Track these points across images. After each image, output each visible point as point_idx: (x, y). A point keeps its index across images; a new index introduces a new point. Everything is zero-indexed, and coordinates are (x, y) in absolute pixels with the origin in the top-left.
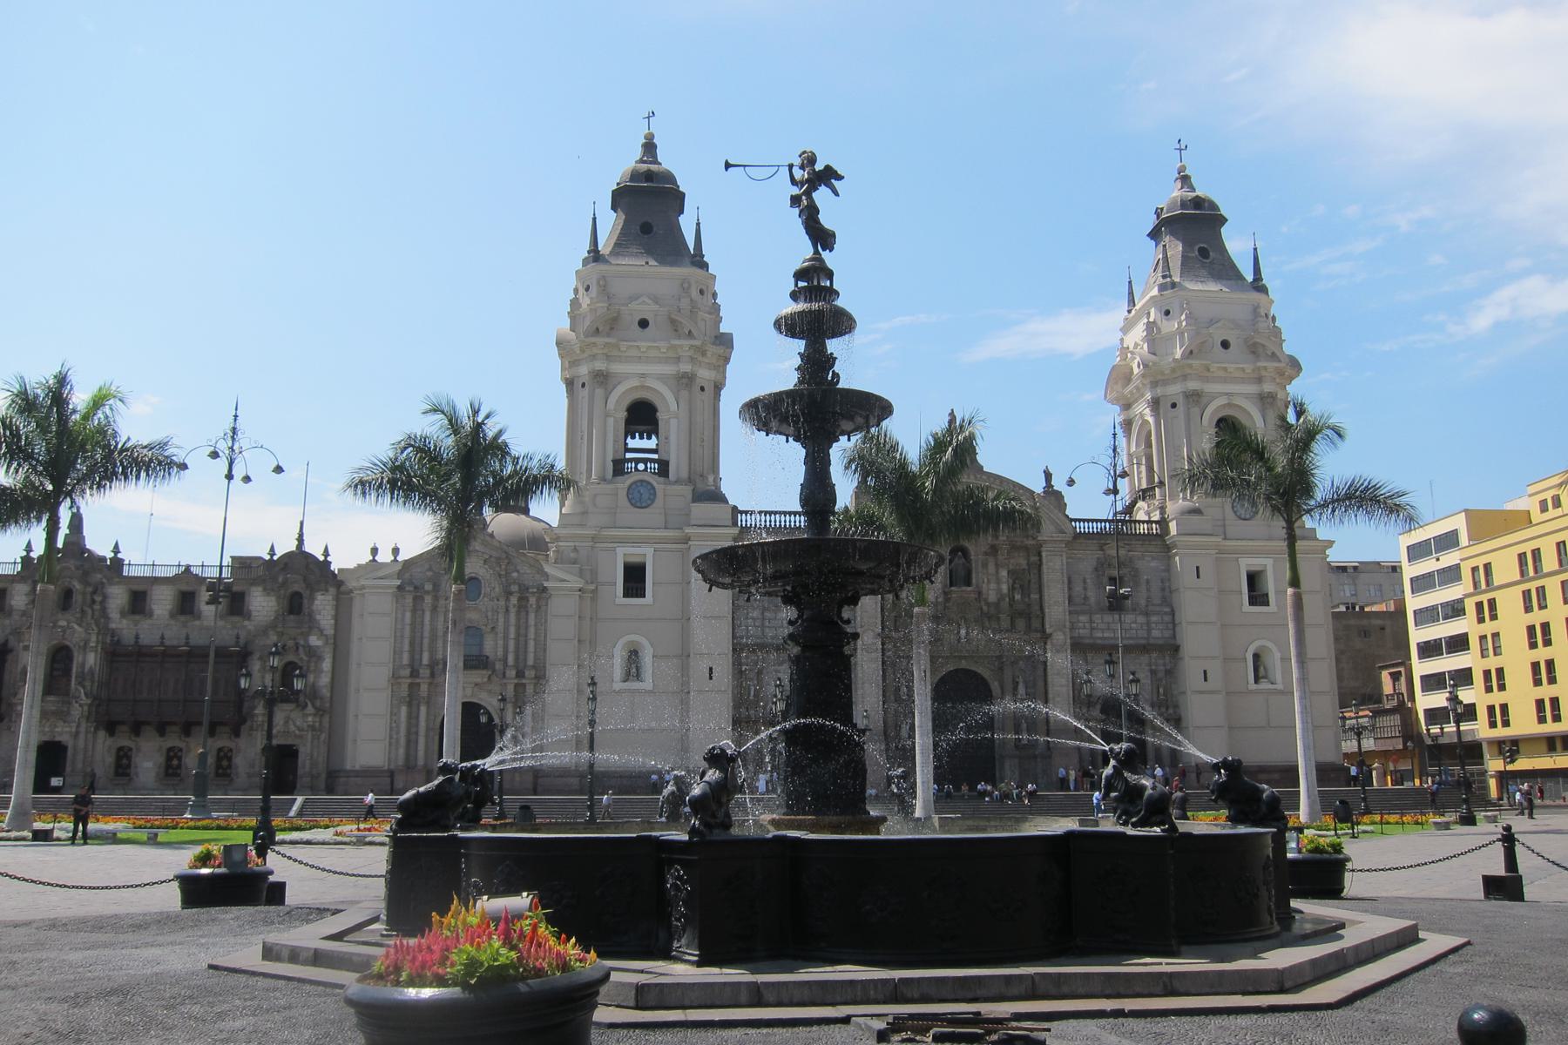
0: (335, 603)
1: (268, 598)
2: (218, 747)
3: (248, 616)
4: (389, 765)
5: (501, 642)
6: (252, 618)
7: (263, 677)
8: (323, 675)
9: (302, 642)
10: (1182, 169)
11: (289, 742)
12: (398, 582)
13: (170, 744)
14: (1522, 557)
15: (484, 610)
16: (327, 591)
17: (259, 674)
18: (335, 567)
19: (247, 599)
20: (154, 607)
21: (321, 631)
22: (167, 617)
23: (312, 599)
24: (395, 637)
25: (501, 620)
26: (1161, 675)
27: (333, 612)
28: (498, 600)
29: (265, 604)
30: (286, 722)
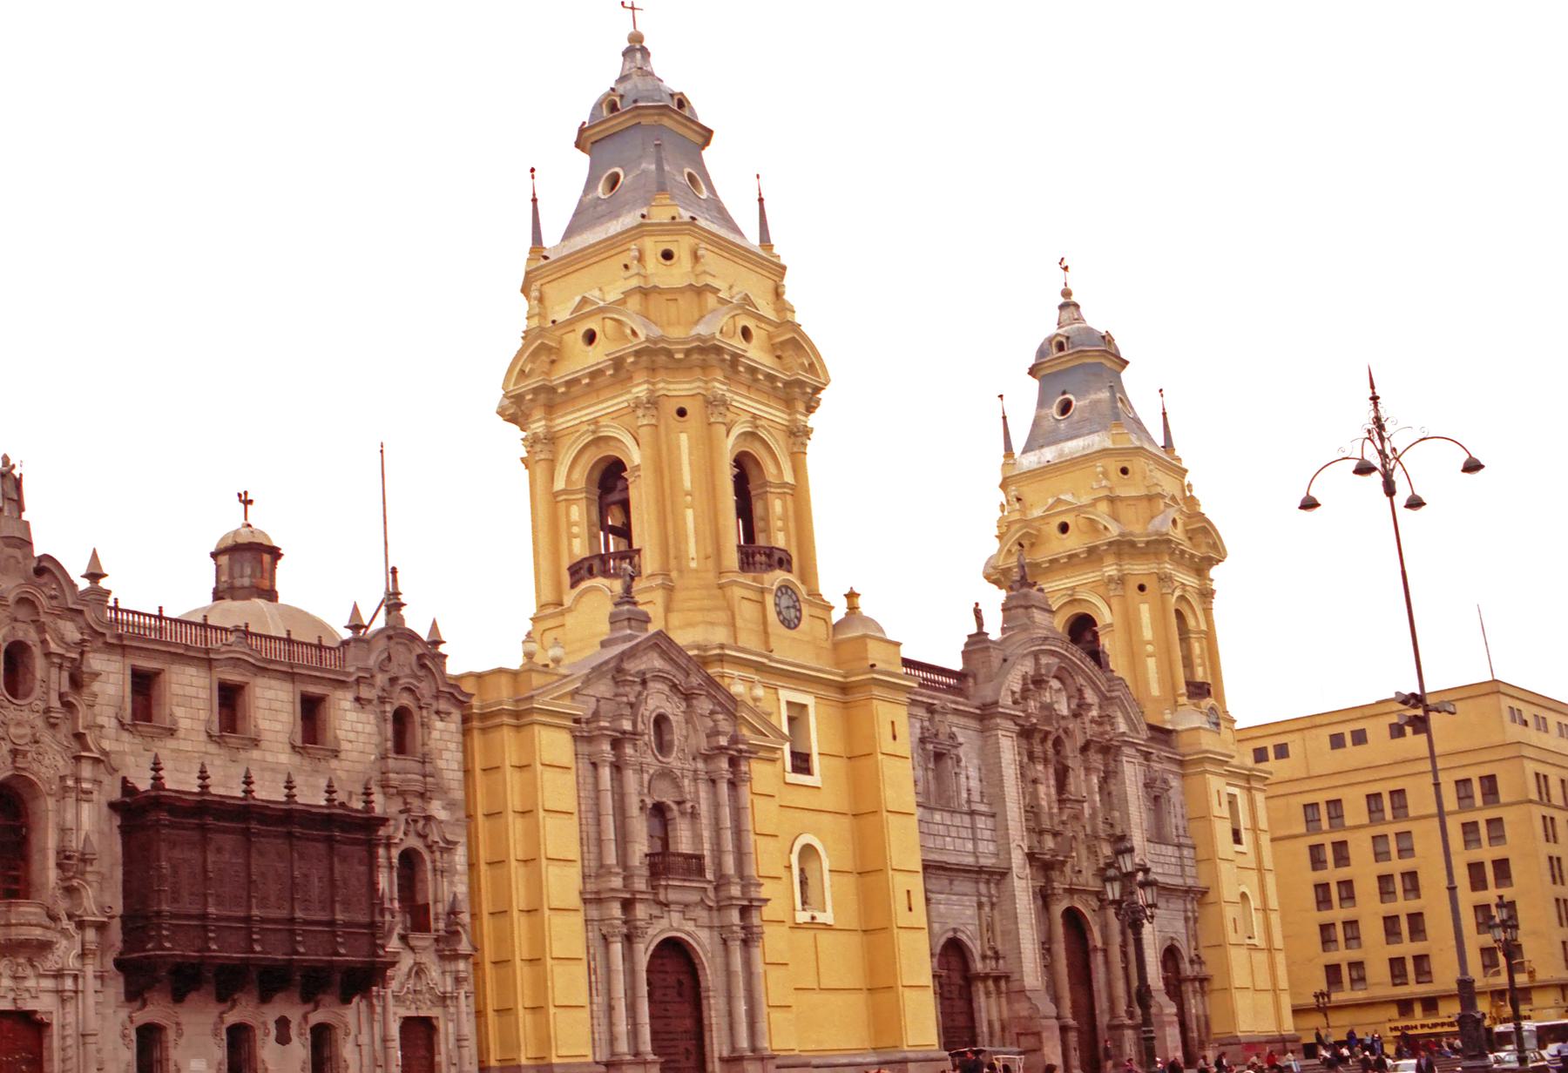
0: (459, 738)
1: (363, 717)
3: (336, 754)
4: (594, 1054)
5: (706, 834)
8: (457, 878)
10: (1066, 293)
11: (422, 1013)
12: (583, 709)
13: (232, 1018)
14: (1311, 807)
18: (453, 668)
20: (179, 712)
21: (443, 791)
24: (580, 811)
25: (703, 795)
26: (1191, 923)
27: (459, 756)
28: (694, 759)
29: (360, 727)
30: (419, 971)
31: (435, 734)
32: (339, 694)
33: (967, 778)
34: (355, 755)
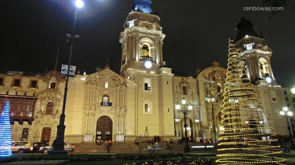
1: (44, 83)
2: (24, 128)
3: (38, 88)
6: (39, 89)
7: (41, 107)
8: (61, 106)
9: (54, 97)
15: (110, 90)
16: (63, 82)
17: (40, 106)
19: (37, 83)
20: (5, 83)
21: (61, 94)
22: (10, 86)
23: (58, 84)
29: (43, 85)
31: (60, 86)
32: (40, 80)
33: (192, 90)
34: (41, 89)
